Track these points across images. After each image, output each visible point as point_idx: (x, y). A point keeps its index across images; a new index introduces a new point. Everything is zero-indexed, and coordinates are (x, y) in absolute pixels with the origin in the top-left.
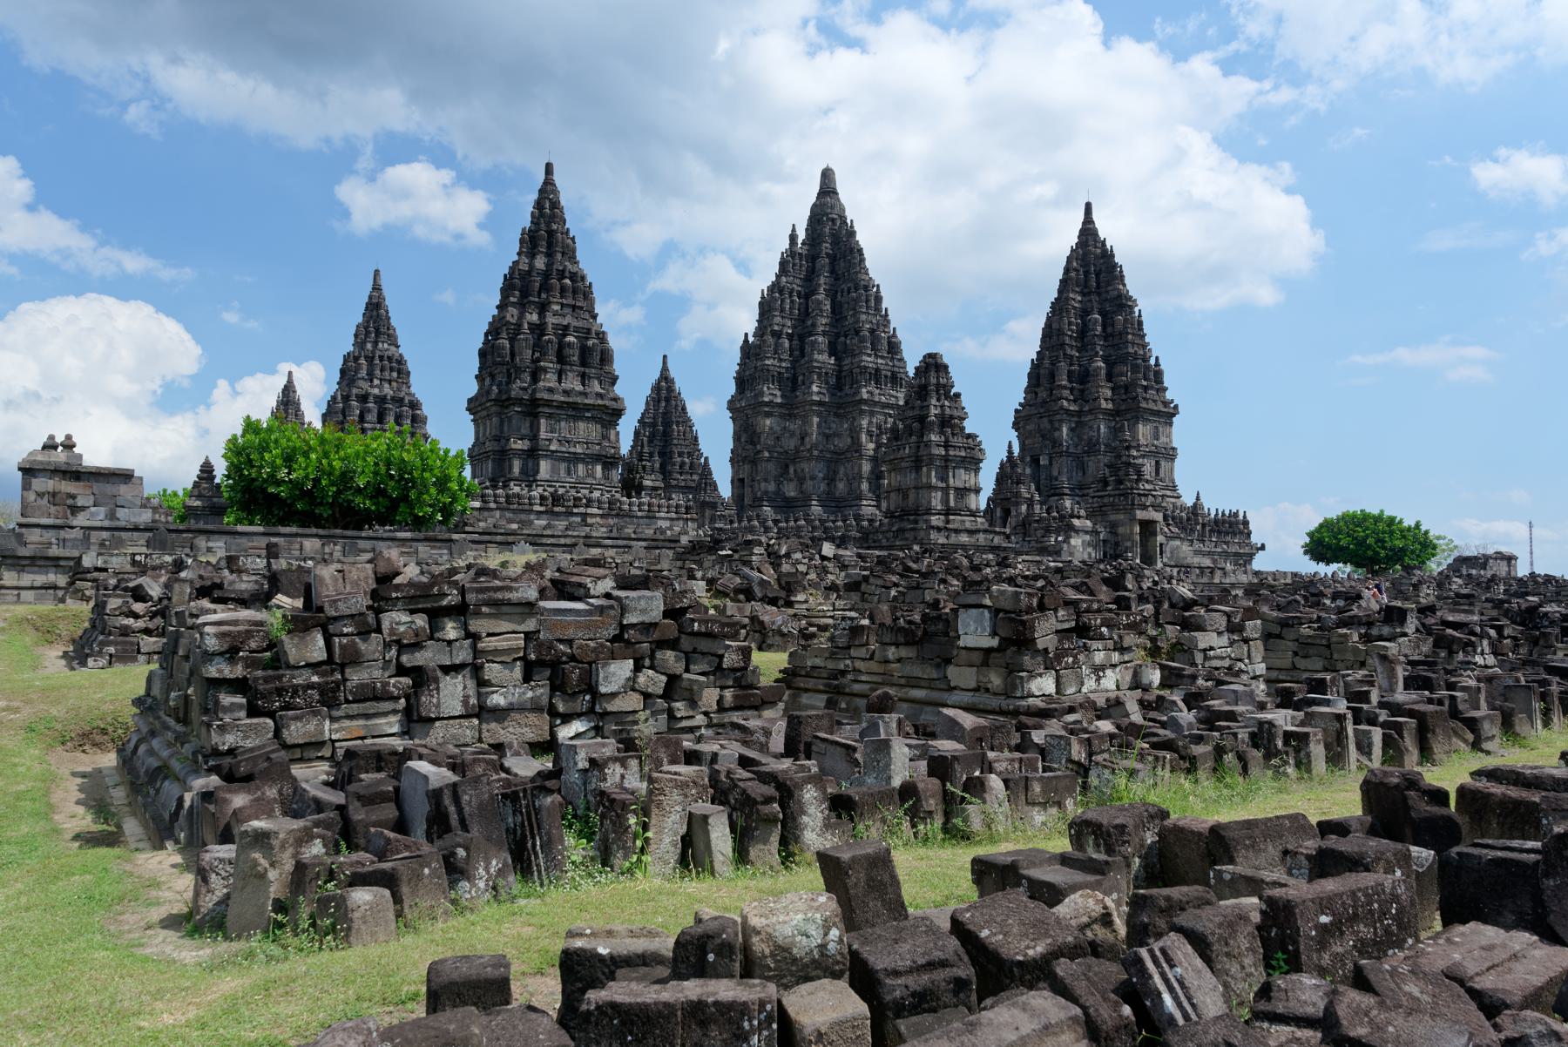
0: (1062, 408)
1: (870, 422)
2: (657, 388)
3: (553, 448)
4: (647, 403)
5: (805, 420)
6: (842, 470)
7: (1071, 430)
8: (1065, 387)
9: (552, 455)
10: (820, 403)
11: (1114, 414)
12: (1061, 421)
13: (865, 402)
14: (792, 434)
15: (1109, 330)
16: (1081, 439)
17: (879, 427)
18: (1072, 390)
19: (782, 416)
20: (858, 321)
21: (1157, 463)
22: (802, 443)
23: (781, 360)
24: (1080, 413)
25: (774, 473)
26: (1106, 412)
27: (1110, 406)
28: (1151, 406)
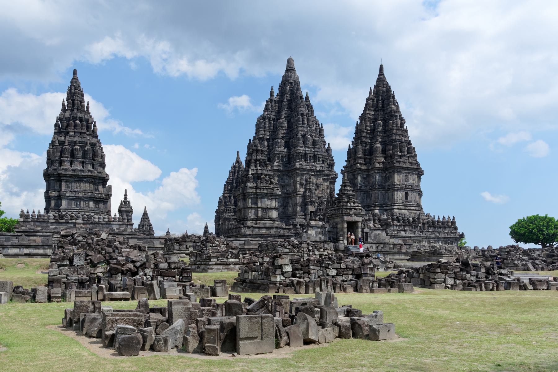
0: (357, 168)
1: (302, 179)
2: (234, 167)
3: (67, 195)
4: (230, 174)
7: (364, 178)
8: (361, 158)
9: (67, 198)
11: (384, 170)
12: (358, 174)
13: (299, 169)
15: (387, 128)
16: (369, 183)
17: (306, 181)
18: (365, 159)
21: (407, 194)
24: (368, 170)
26: (379, 169)
27: (381, 166)
28: (402, 165)
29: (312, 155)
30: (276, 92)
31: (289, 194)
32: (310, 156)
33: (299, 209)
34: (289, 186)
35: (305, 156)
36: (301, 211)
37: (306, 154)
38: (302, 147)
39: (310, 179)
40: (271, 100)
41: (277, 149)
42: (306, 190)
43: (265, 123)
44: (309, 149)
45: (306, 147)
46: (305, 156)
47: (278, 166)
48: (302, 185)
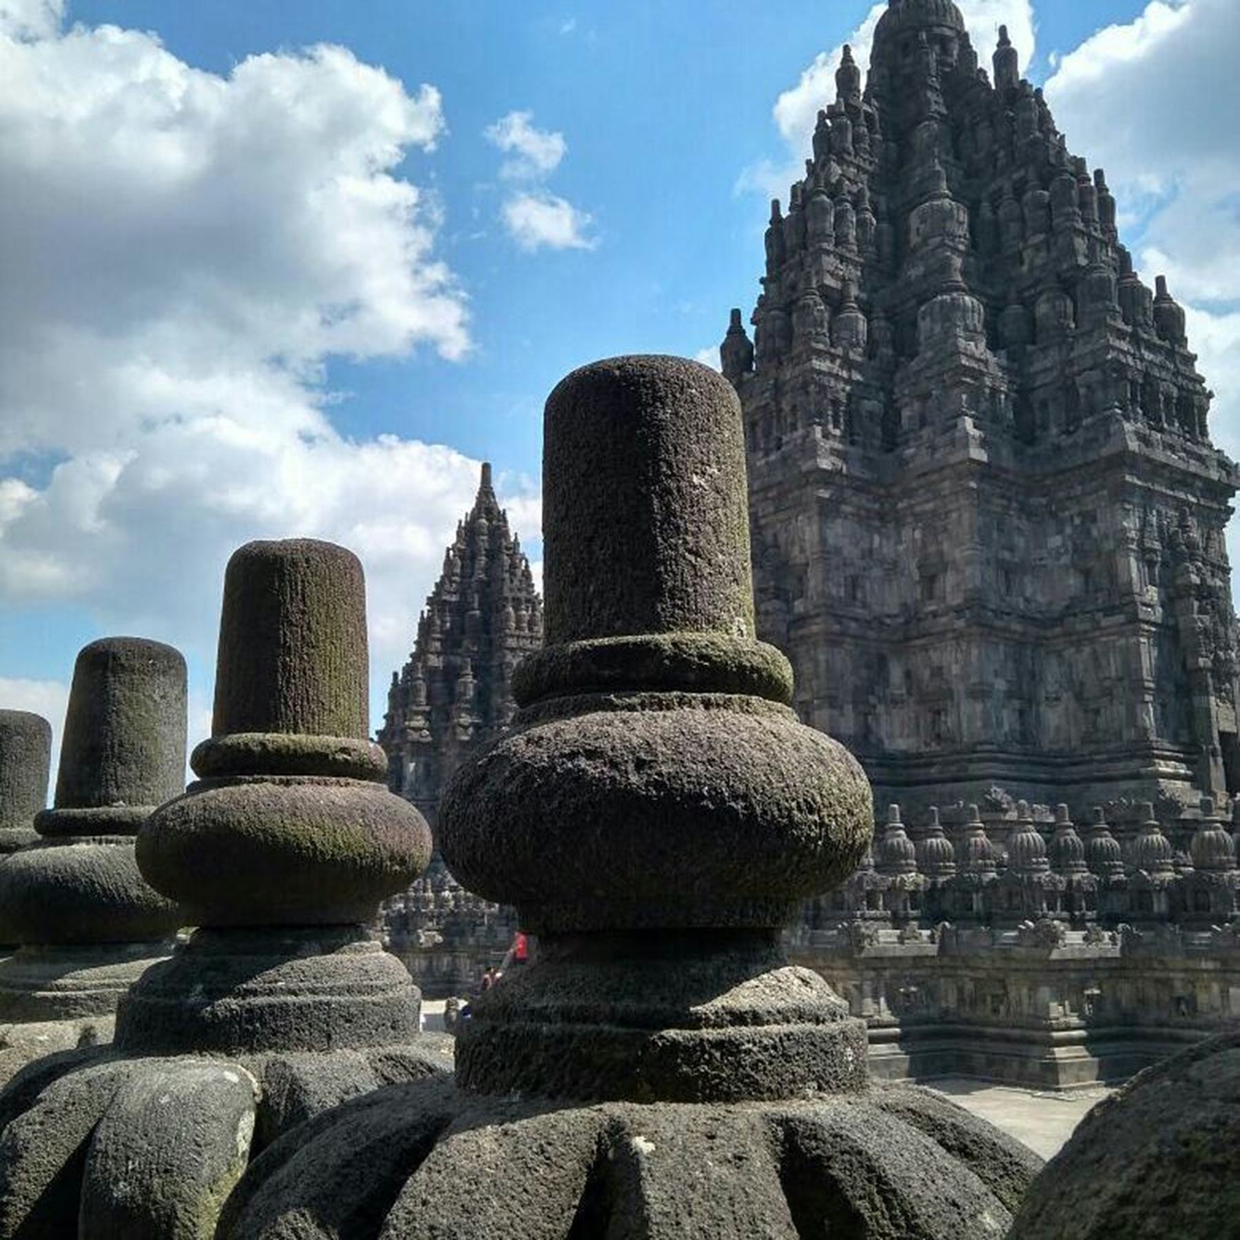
1: (1145, 524)
5: (933, 524)
6: (1052, 673)
14: (893, 568)
17: (1170, 542)
20: (1073, 252)
22: (929, 594)
25: (851, 680)
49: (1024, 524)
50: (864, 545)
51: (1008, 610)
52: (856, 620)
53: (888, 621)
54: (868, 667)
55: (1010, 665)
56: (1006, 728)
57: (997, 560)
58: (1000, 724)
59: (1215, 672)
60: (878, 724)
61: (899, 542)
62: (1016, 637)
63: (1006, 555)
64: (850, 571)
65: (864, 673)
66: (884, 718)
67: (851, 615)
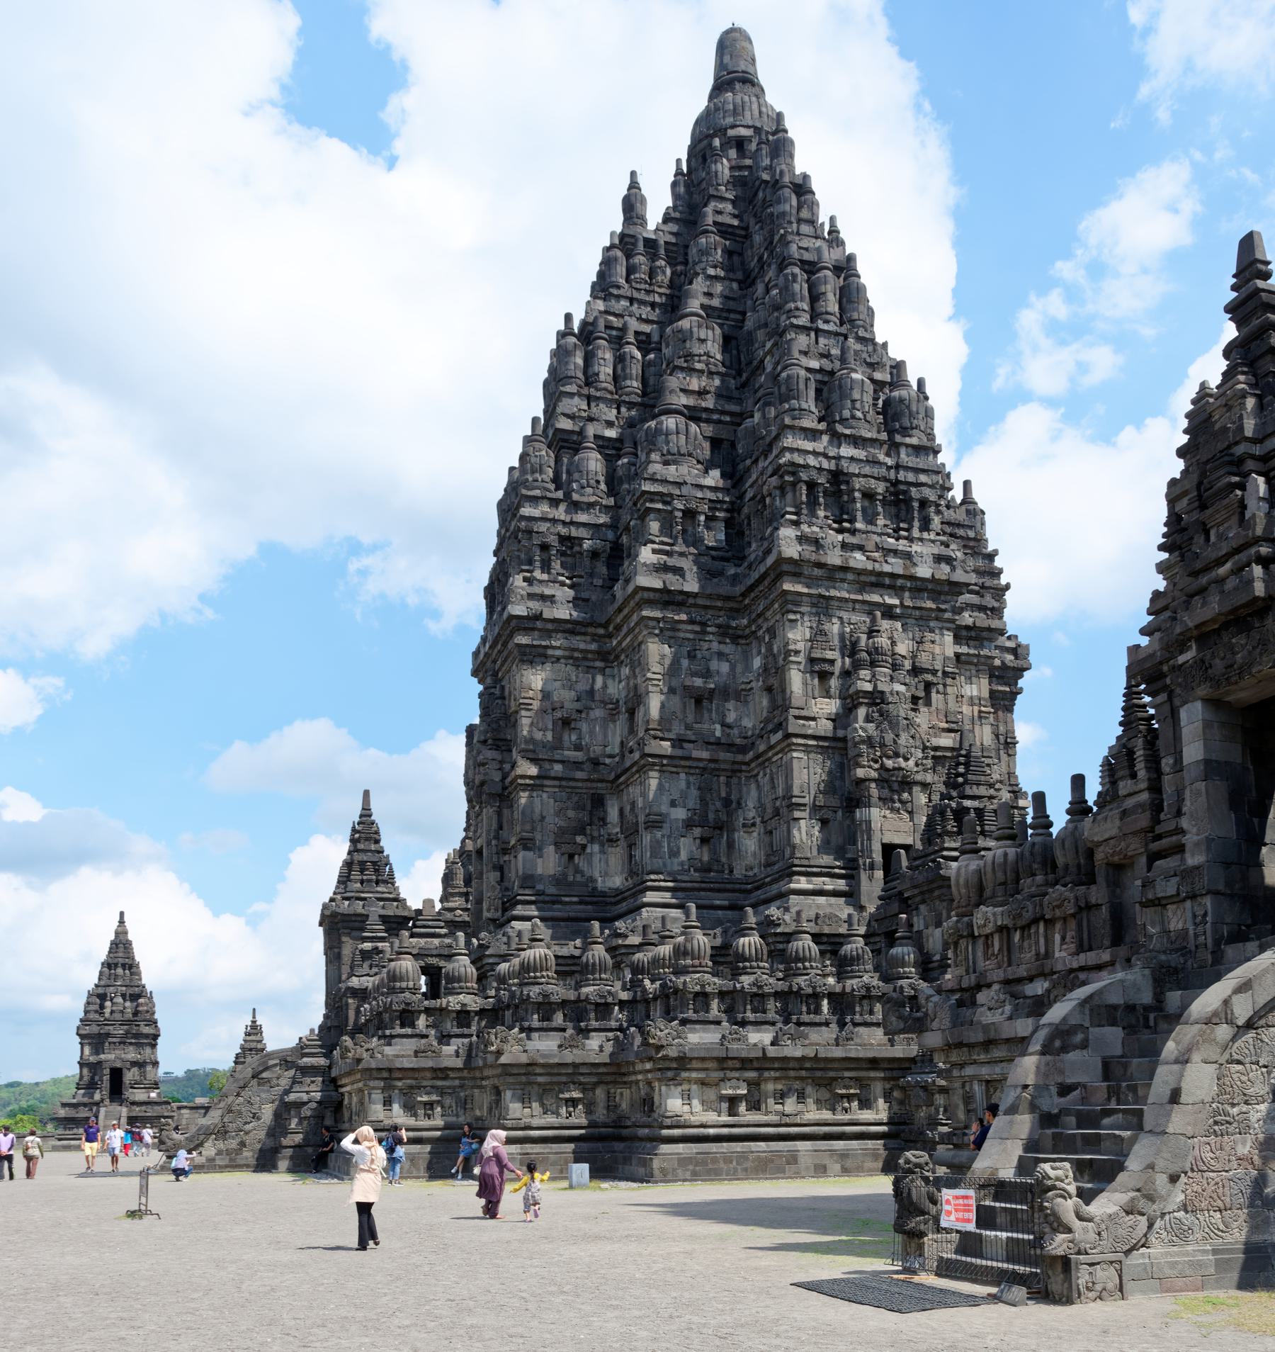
1: (818, 635)
10: (668, 599)
13: (795, 569)
17: (850, 648)
19: (577, 660)
23: (575, 506)
25: (553, 822)
29: (880, 488)
30: (658, 202)
31: (743, 750)
32: (869, 495)
33: (806, 833)
34: (741, 696)
35: (836, 491)
36: (824, 847)
37: (837, 477)
38: (813, 434)
39: (872, 633)
40: (625, 243)
41: (656, 468)
42: (850, 702)
43: (589, 358)
44: (860, 454)
45: (837, 438)
46: (836, 491)
47: (663, 568)
48: (824, 676)
49: (728, 649)
50: (583, 686)
51: (693, 738)
52: (562, 762)
53: (608, 761)
54: (579, 807)
55: (694, 793)
56: (684, 856)
57: (685, 688)
58: (674, 853)
59: (881, 782)
60: (590, 864)
61: (620, 682)
62: (701, 765)
63: (698, 682)
64: (558, 714)
65: (571, 814)
66: (596, 858)
67: (557, 757)
